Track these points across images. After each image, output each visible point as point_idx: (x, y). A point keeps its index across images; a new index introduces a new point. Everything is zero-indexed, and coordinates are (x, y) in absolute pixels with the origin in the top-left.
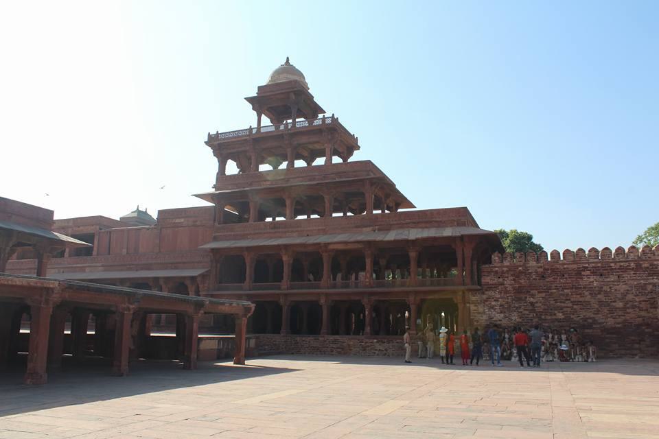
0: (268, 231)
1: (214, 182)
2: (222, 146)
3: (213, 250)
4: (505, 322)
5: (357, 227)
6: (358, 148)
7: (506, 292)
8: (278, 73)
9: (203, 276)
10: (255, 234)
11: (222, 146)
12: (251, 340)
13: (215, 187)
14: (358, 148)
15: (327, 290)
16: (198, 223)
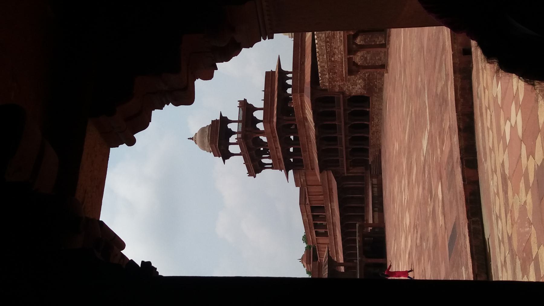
0: (307, 153)
1: (278, 171)
2: (255, 167)
3: (321, 171)
4: (362, 85)
5: (305, 127)
6: (245, 100)
7: (344, 84)
8: (203, 147)
9: (335, 173)
10: (310, 157)
11: (255, 167)
12: (374, 183)
13: (281, 170)
14: (245, 100)
15: (343, 136)
16: (304, 174)
